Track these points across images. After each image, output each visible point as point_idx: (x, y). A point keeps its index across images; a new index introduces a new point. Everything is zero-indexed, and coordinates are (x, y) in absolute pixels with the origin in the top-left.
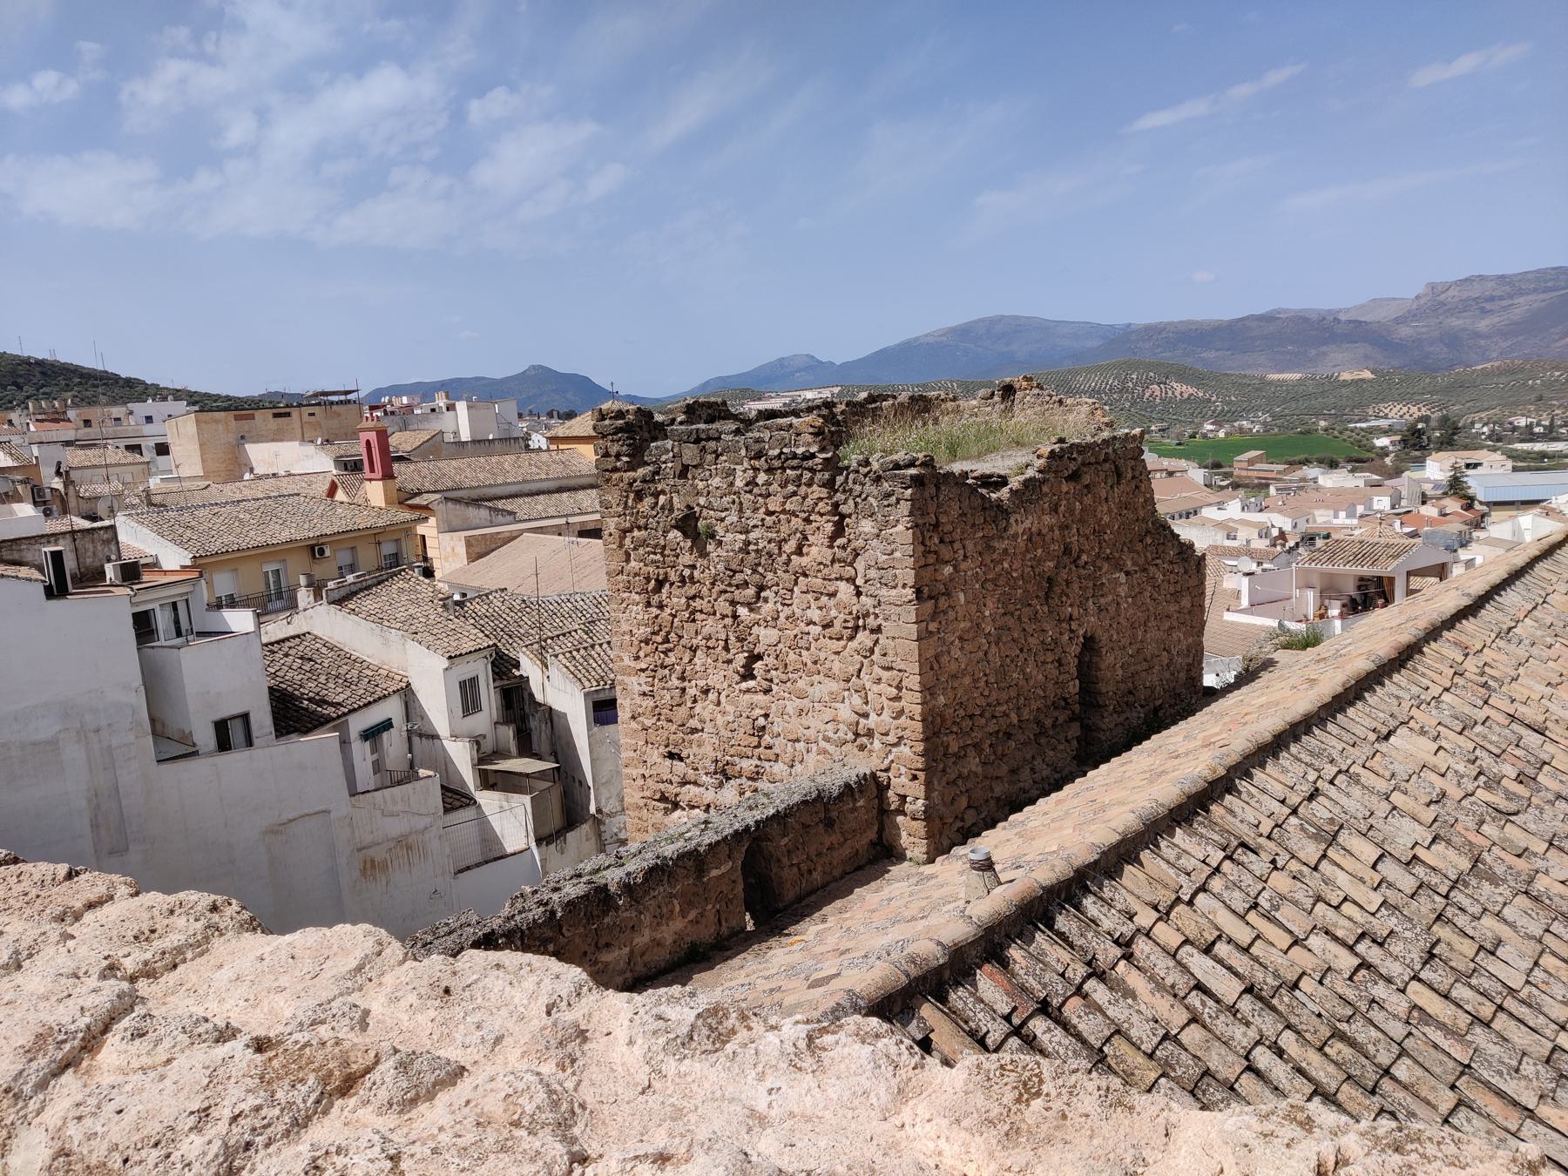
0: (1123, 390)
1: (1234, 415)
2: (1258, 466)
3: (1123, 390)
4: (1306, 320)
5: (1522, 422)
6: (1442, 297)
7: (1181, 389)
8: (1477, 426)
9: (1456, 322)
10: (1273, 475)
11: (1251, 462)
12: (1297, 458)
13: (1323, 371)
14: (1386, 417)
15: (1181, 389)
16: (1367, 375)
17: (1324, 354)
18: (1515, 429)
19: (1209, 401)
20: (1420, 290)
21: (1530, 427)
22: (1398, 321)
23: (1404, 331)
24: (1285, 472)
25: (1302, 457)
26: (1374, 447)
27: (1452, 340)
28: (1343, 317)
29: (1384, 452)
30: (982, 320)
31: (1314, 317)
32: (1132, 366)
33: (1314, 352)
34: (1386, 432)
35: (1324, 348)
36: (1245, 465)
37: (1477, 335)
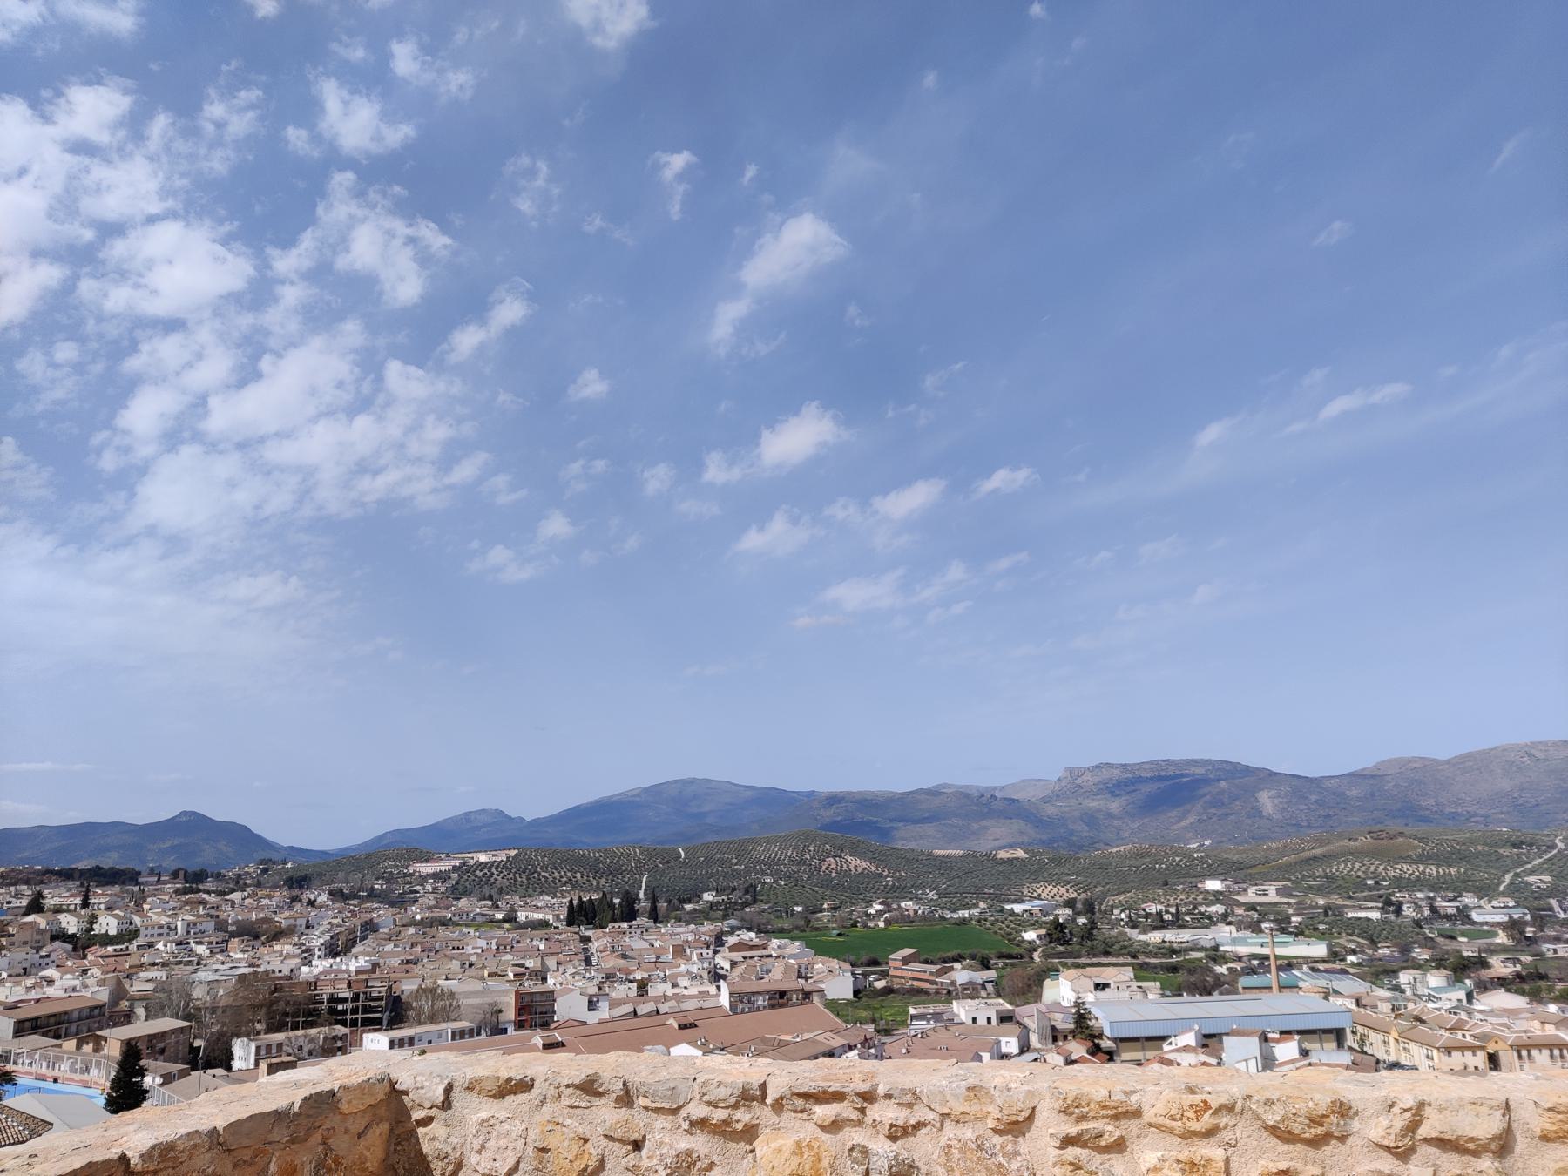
0: (802, 862)
1: (901, 891)
2: (912, 966)
3: (802, 862)
4: (967, 796)
5: (1153, 908)
6: (1079, 781)
7: (856, 863)
8: (1116, 912)
9: (1092, 804)
10: (926, 976)
11: (906, 961)
12: (950, 954)
13: (983, 846)
14: (1039, 898)
15: (856, 863)
16: (1021, 854)
17: (985, 828)
18: (1148, 915)
19: (881, 875)
20: (1061, 774)
21: (1159, 914)
22: (1046, 800)
23: (1050, 810)
24: (939, 973)
25: (955, 953)
26: (1023, 941)
27: (1090, 819)
28: (998, 794)
29: (1032, 948)
30: (675, 782)
31: (975, 793)
32: (808, 838)
33: (975, 826)
34: (1034, 925)
35: (984, 823)
36: (899, 964)
37: (1110, 816)
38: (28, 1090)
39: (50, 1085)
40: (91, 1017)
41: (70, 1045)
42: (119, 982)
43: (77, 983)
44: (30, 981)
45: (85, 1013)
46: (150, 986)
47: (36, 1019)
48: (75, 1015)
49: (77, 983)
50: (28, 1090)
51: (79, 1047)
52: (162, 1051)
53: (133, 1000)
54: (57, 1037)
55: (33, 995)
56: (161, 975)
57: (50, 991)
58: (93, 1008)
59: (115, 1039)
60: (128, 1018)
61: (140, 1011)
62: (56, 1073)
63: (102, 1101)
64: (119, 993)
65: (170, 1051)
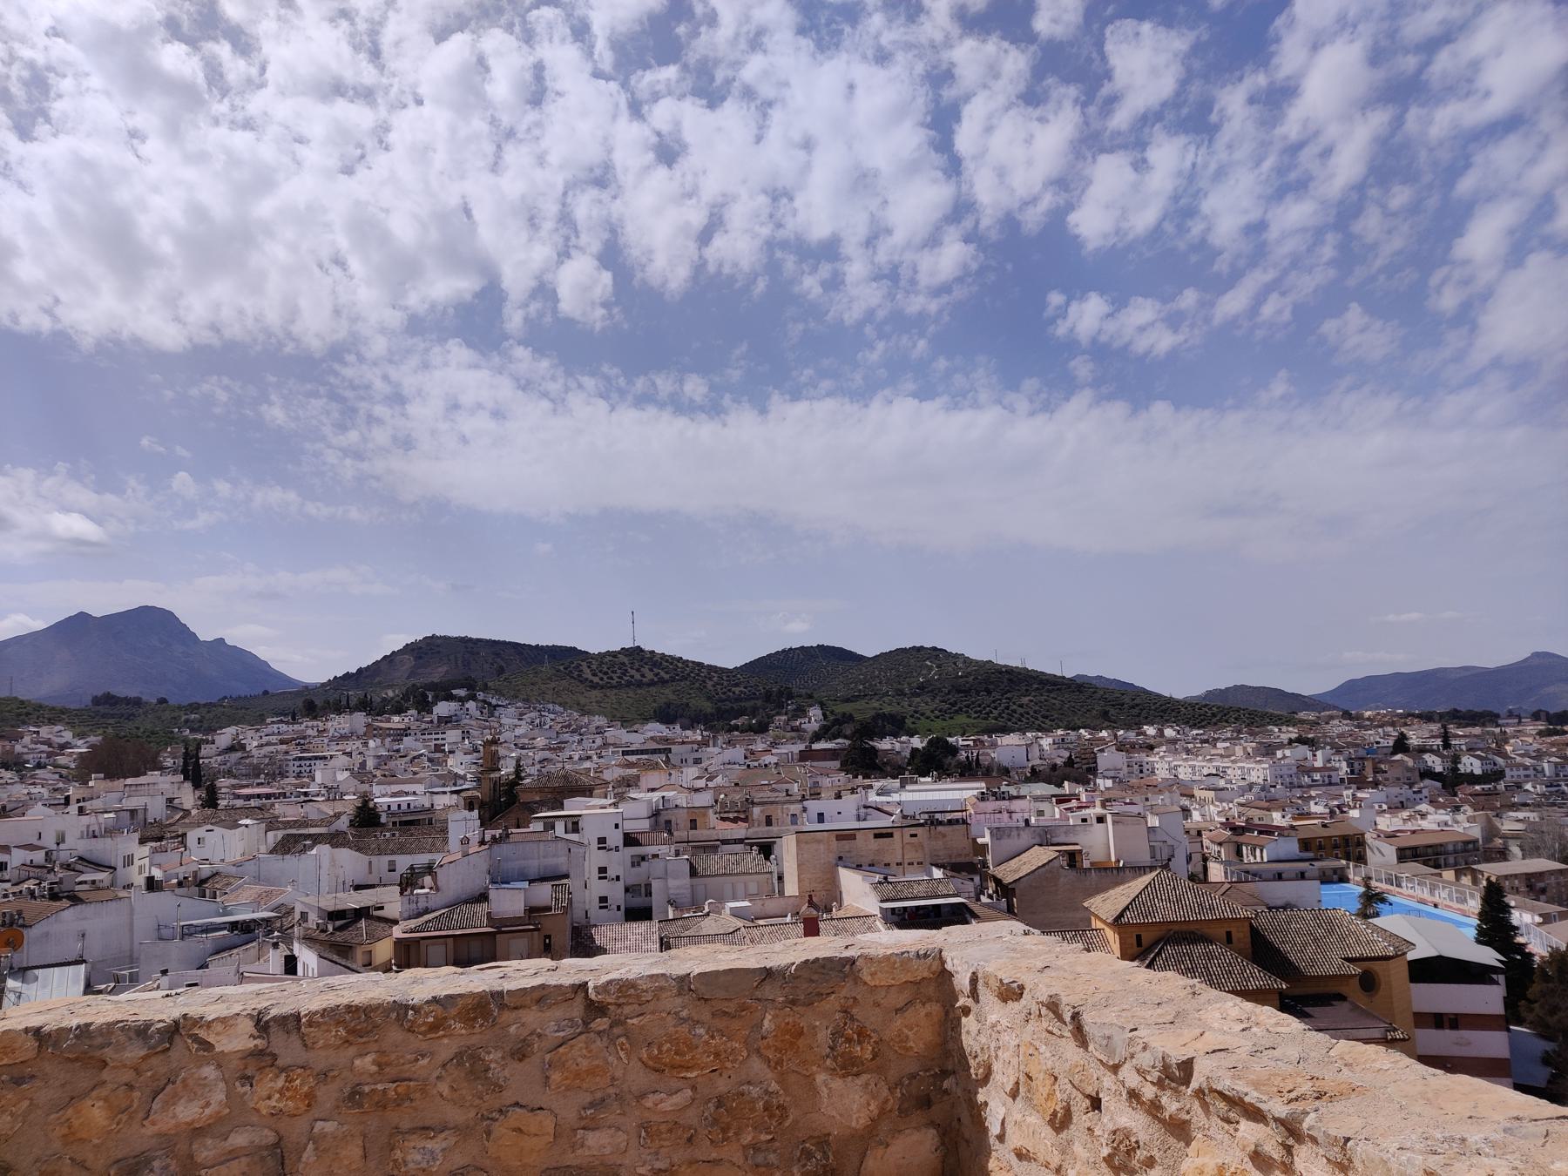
38: (1408, 911)
39: (1431, 909)
40: (1466, 851)
41: (1449, 875)
42: (1489, 821)
43: (1447, 818)
44: (1405, 814)
45: (1460, 847)
46: (1520, 826)
47: (1415, 848)
48: (1450, 848)
49: (1447, 818)
50: (1408, 911)
51: (1458, 878)
52: (1543, 891)
53: (1504, 837)
54: (1437, 866)
55: (1410, 826)
56: (1533, 816)
57: (1424, 824)
58: (1466, 843)
59: (1493, 870)
60: (1503, 855)
61: (1515, 849)
62: (1436, 899)
63: (1473, 933)
64: (1491, 832)
65: (1552, 892)
